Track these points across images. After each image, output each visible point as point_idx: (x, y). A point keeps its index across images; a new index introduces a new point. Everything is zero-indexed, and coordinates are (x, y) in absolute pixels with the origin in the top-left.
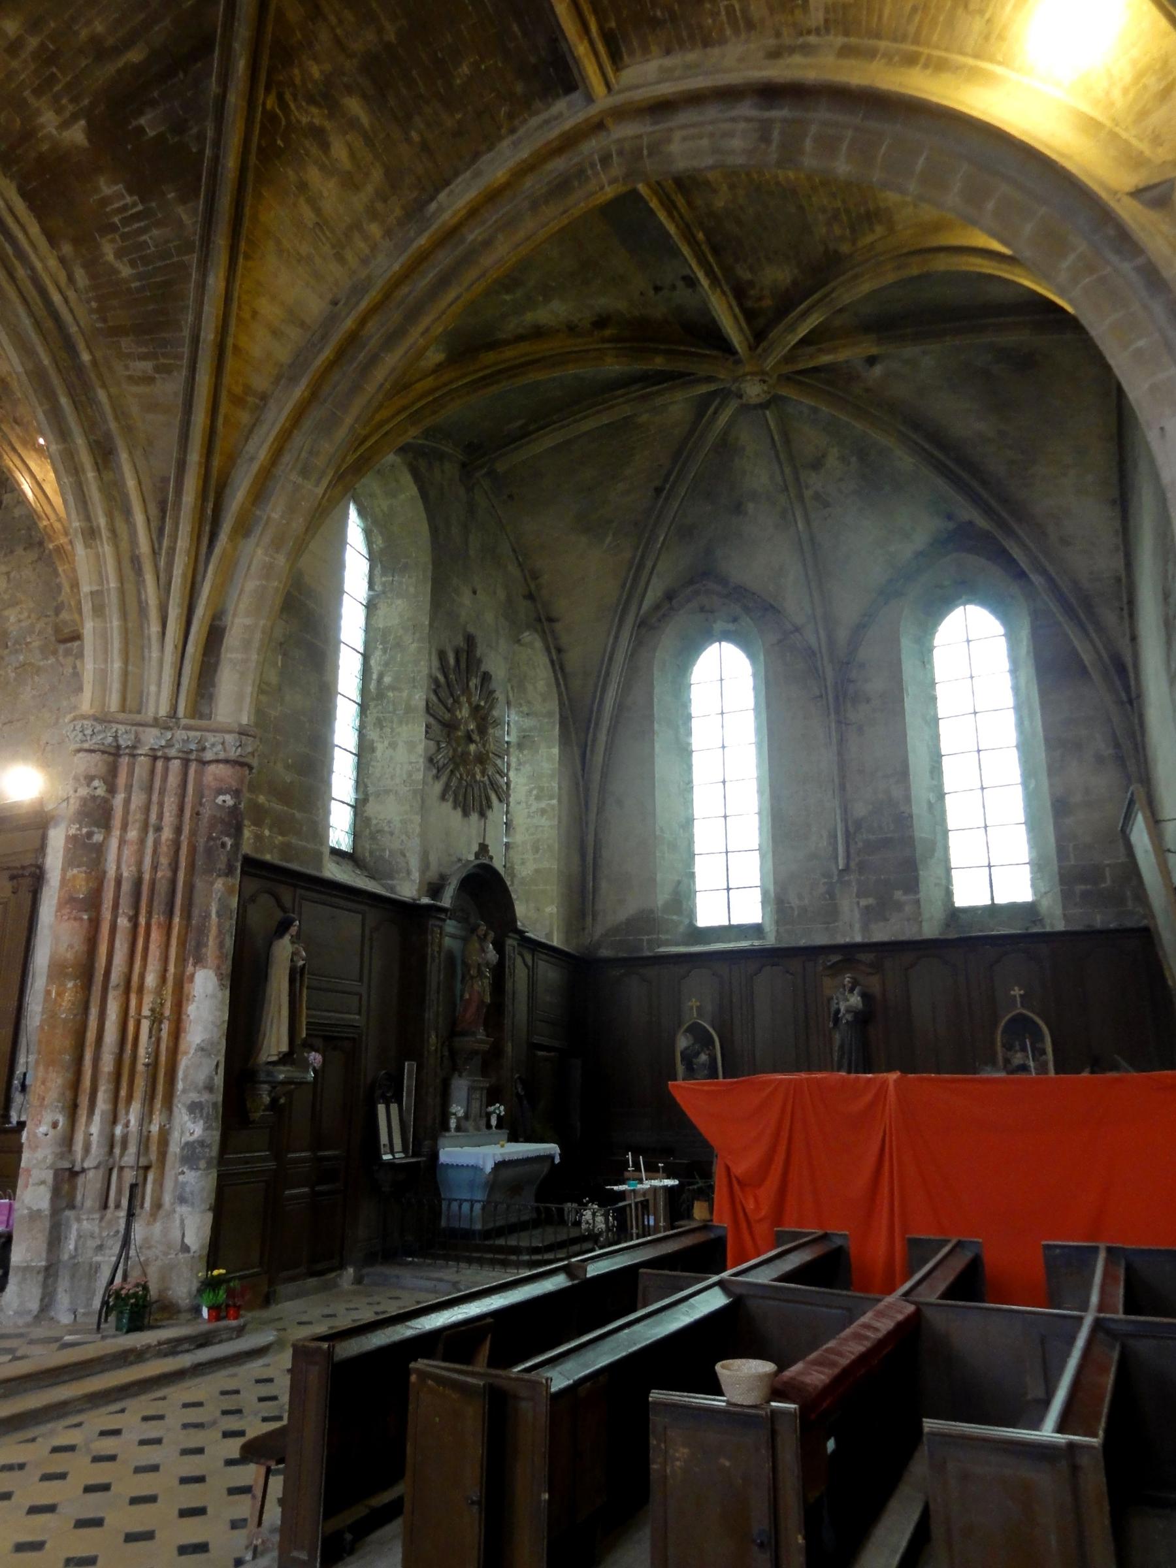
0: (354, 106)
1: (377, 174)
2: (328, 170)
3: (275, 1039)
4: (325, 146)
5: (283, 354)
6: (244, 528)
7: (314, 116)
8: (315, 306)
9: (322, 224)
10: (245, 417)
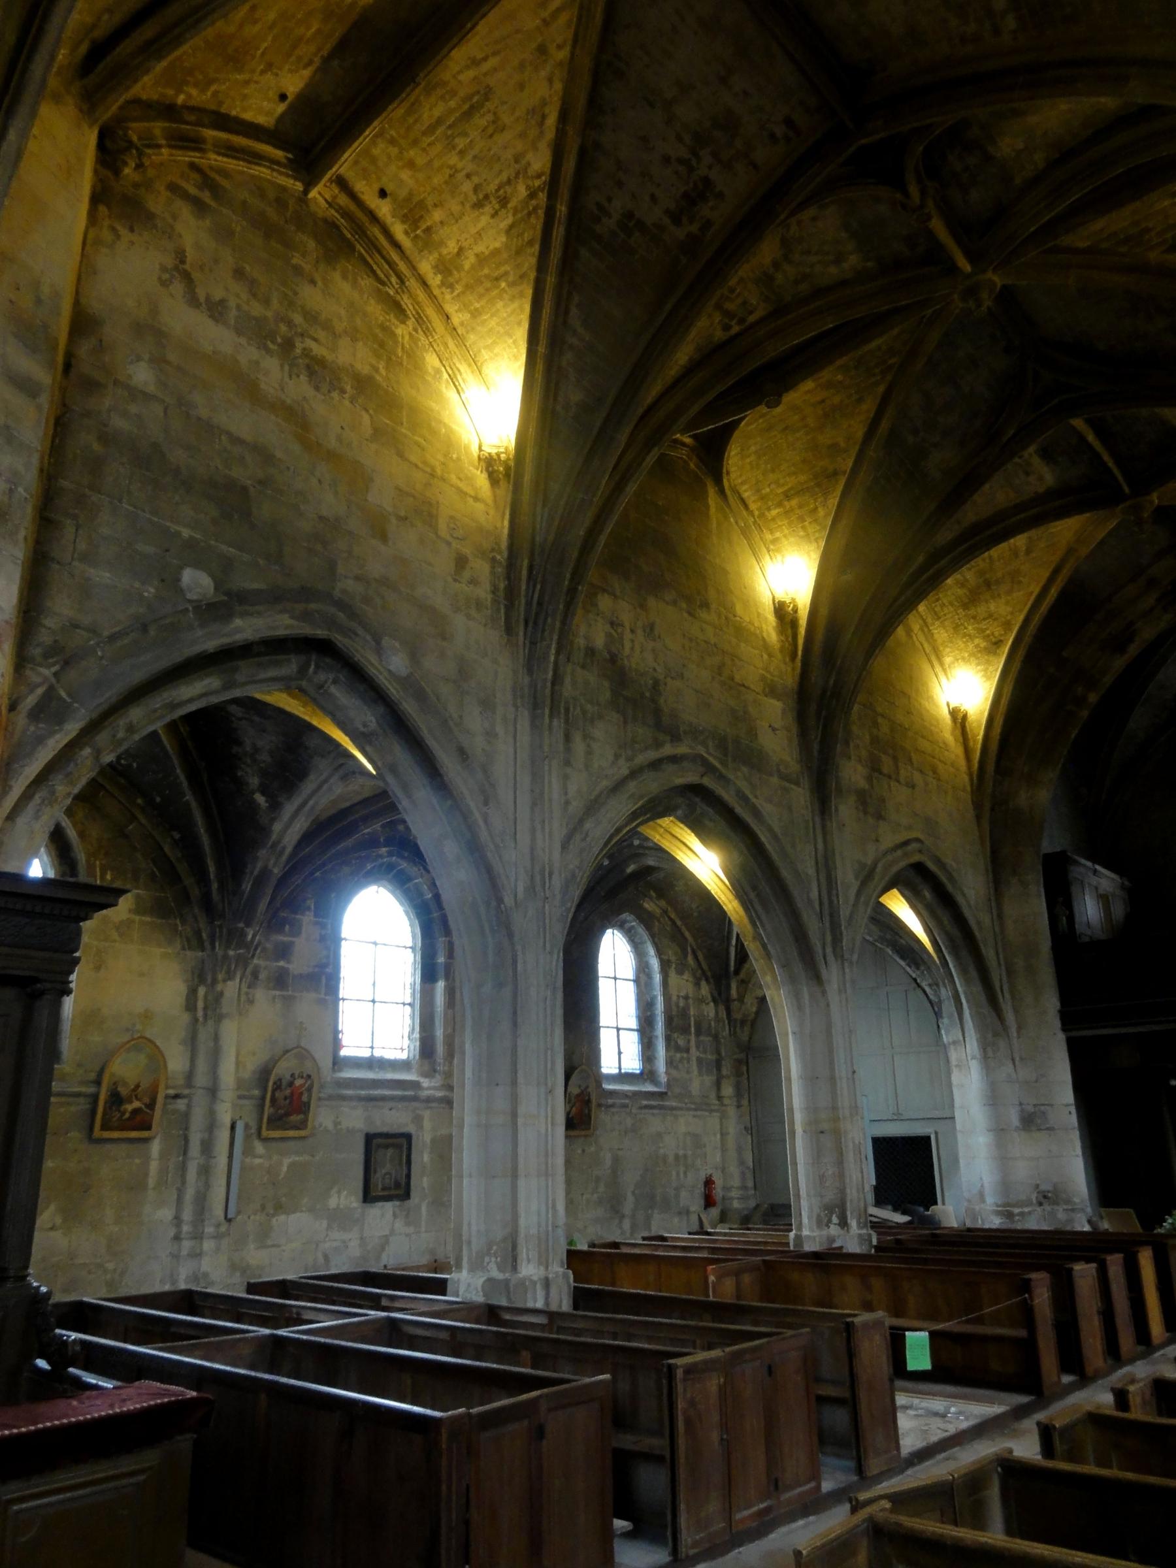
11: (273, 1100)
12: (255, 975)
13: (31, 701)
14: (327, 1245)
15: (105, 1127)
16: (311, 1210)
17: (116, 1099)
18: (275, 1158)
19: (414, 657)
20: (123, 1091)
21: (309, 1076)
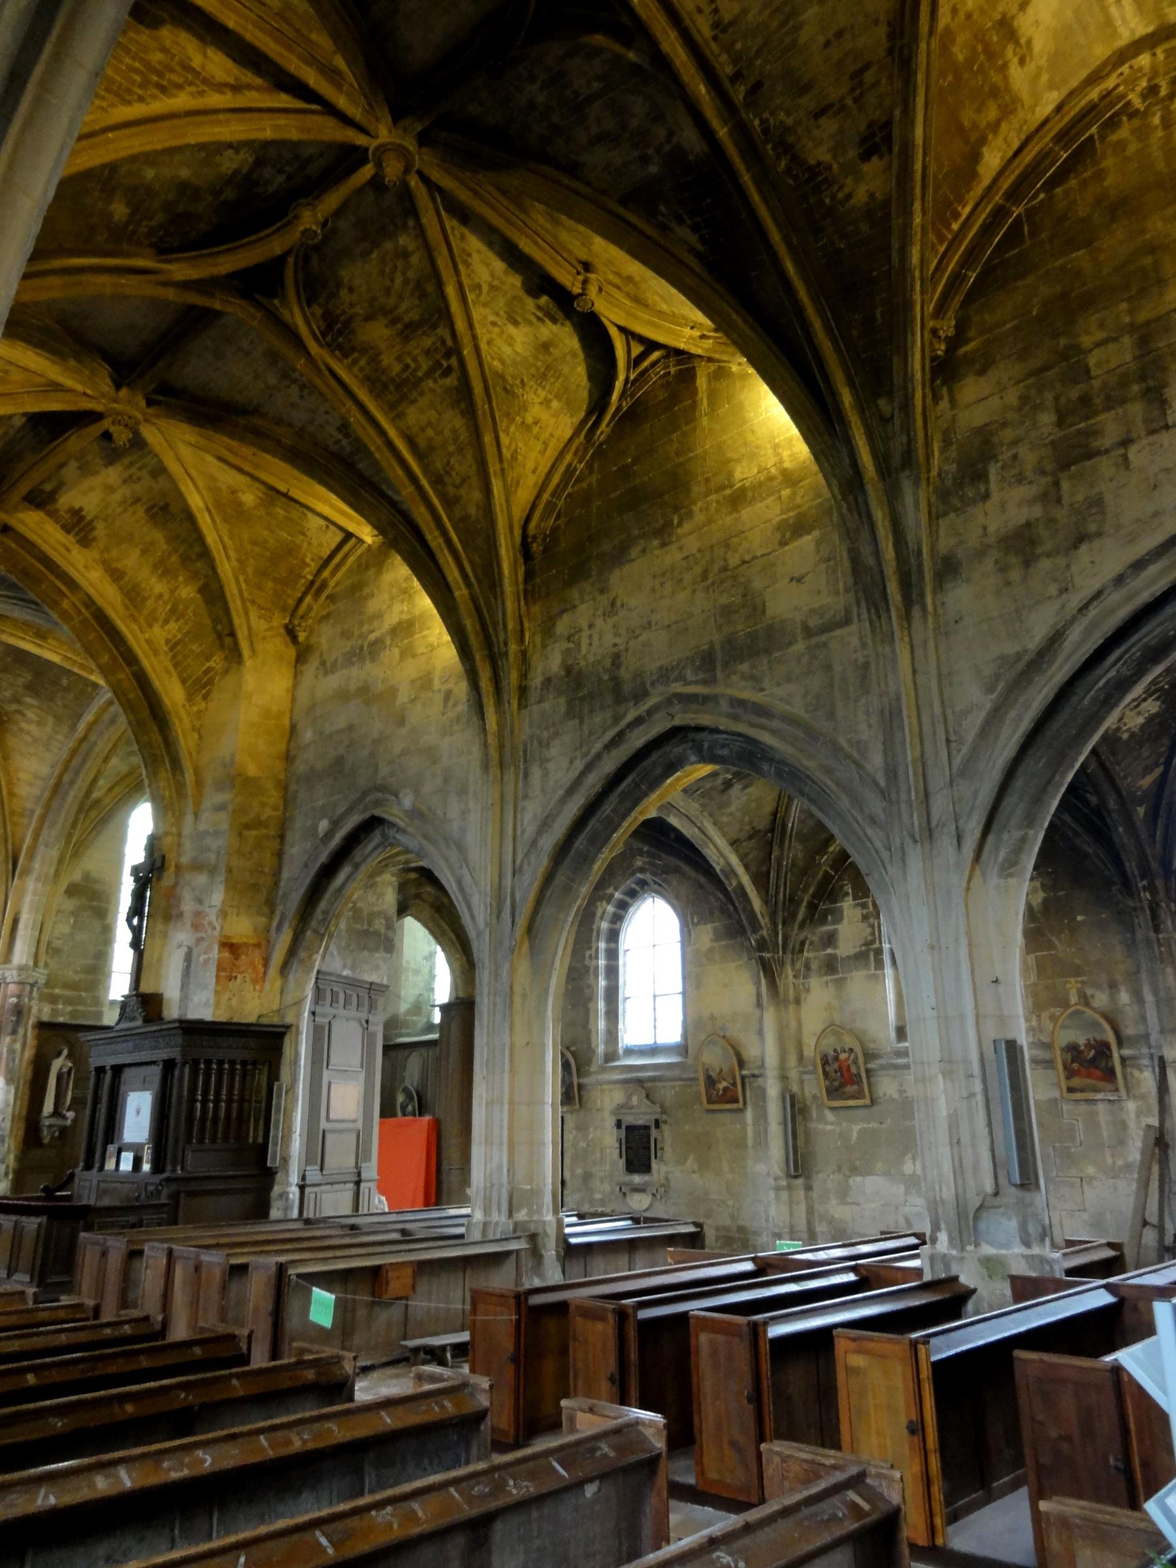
0: (28, 700)
1: (51, 719)
2: (29, 722)
3: (48, 1106)
4: (23, 715)
5: (35, 791)
6: (27, 871)
7: (15, 707)
8: (45, 770)
9: (36, 740)
10: (25, 821)
11: (826, 1074)
12: (807, 967)
13: (275, 924)
14: (907, 1209)
15: (737, 1101)
16: (886, 1174)
17: (711, 1082)
18: (844, 1124)
19: (417, 792)
20: (714, 1075)
21: (851, 1050)
